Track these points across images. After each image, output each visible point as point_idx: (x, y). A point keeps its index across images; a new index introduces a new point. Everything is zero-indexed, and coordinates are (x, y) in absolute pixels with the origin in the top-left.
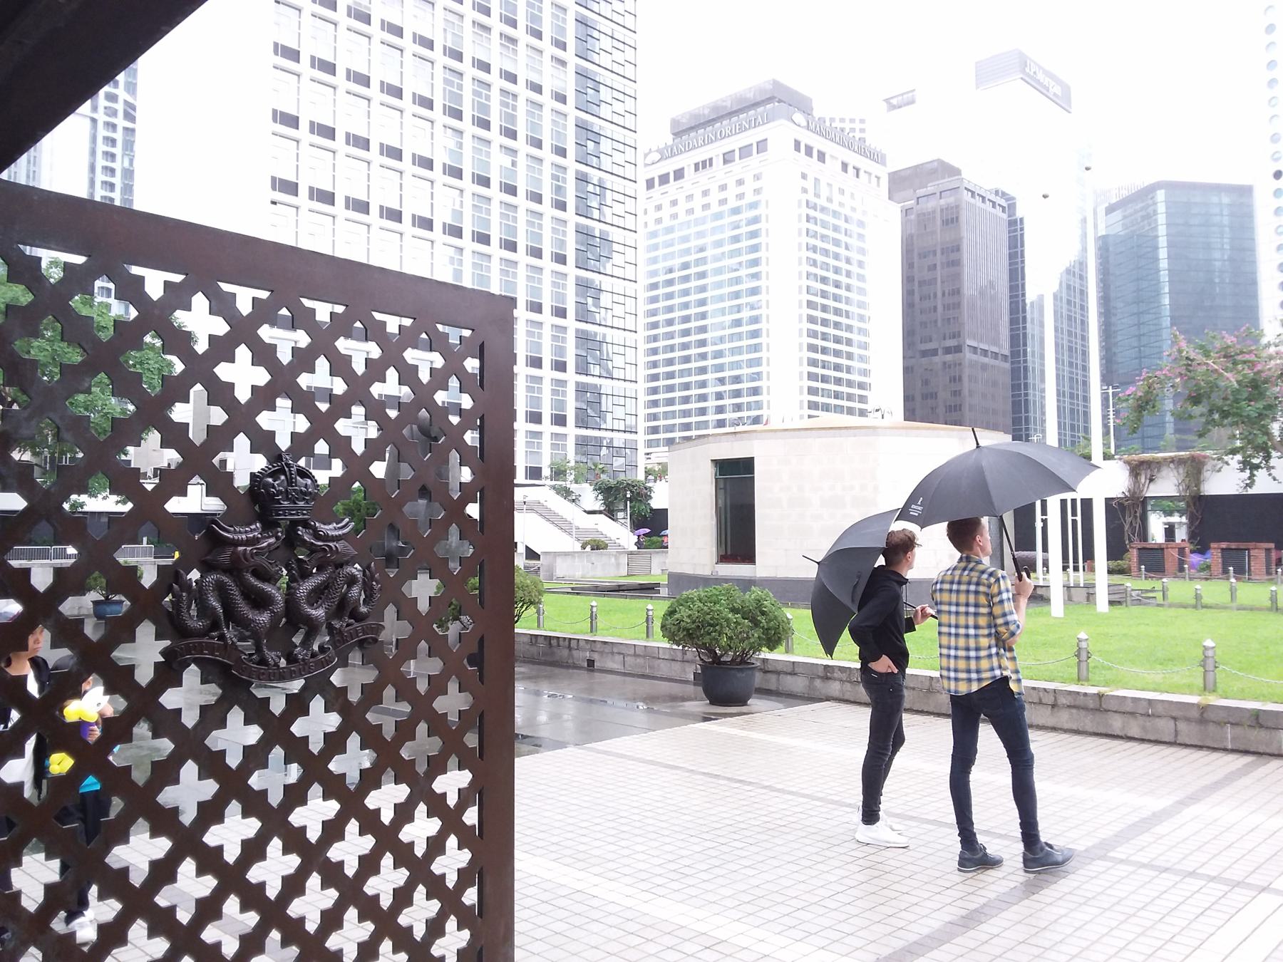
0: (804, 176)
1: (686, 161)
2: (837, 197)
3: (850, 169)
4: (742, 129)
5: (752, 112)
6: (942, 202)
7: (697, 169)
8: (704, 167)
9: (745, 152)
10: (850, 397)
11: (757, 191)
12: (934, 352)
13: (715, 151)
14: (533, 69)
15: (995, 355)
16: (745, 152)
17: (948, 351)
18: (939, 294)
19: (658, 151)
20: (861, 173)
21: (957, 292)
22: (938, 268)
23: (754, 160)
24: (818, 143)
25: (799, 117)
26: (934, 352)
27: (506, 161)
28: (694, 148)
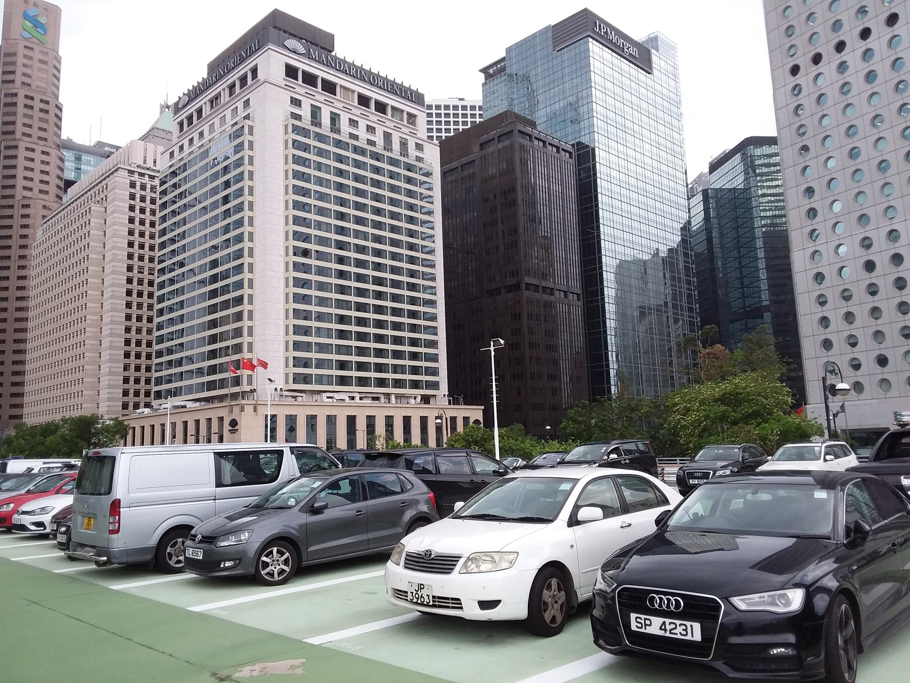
0: (296, 102)
1: (203, 101)
4: (242, 60)
6: (500, 146)
7: (212, 107)
9: (243, 80)
11: (247, 117)
12: (497, 292)
13: (221, 87)
17: (509, 289)
19: (188, 95)
21: (515, 231)
22: (499, 208)
24: (322, 73)
25: (291, 43)
26: (497, 292)
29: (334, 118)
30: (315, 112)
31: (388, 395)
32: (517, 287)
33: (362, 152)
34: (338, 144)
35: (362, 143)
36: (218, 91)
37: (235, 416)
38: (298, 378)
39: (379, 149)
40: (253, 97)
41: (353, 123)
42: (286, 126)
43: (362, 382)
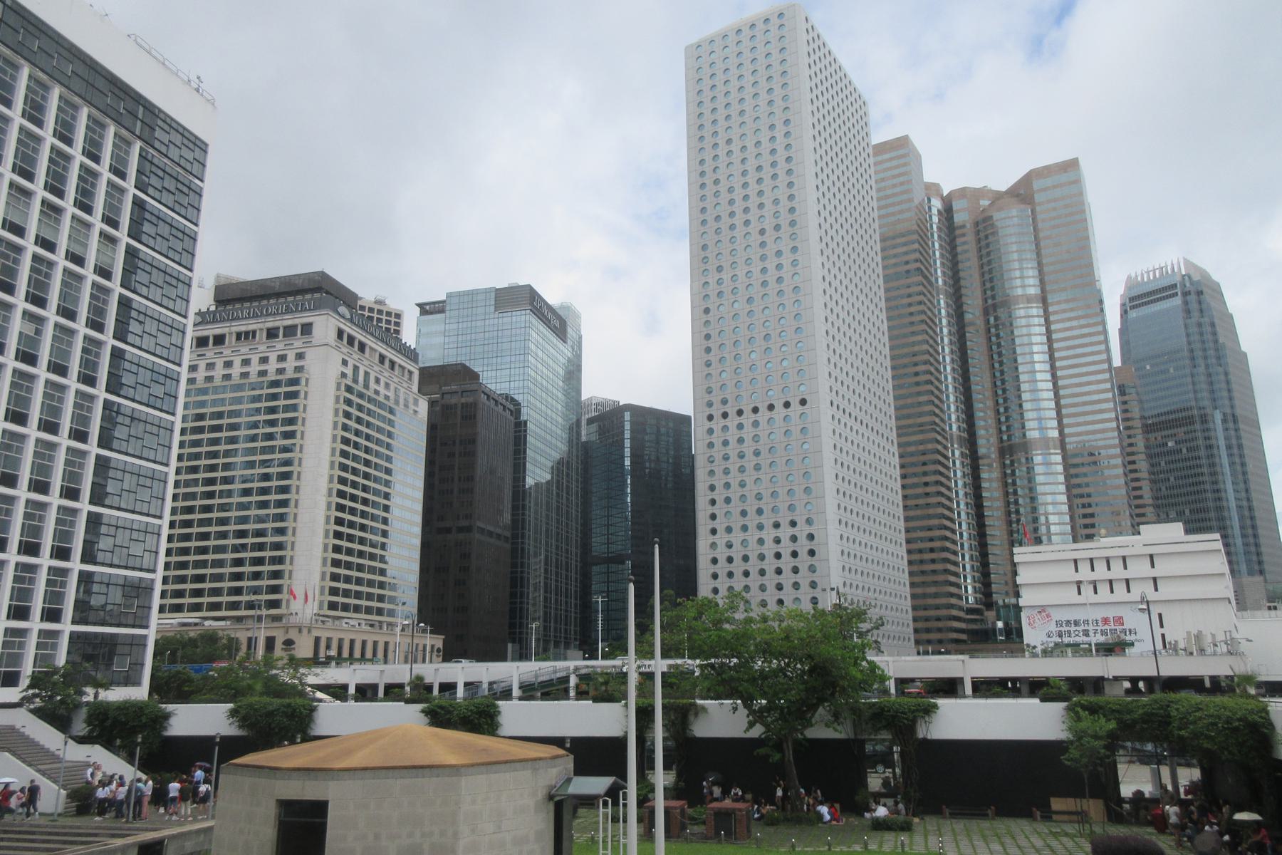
0: (345, 363)
2: (372, 385)
3: (387, 363)
4: (288, 311)
5: (299, 297)
8: (247, 337)
9: (290, 331)
10: (370, 597)
11: (299, 369)
12: (448, 530)
14: (76, 241)
15: (499, 536)
16: (290, 331)
17: (461, 530)
18: (456, 478)
20: (397, 367)
21: (470, 479)
23: (298, 343)
24: (359, 336)
26: (448, 530)
27: (30, 329)
28: (238, 318)
29: (367, 374)
30: (356, 368)
31: (380, 622)
32: (469, 529)
33: (381, 406)
34: (370, 400)
35: (381, 399)
36: (251, 328)
37: (293, 635)
38: (333, 606)
39: (391, 403)
40: (311, 354)
41: (377, 381)
42: (339, 385)
43: (369, 610)
